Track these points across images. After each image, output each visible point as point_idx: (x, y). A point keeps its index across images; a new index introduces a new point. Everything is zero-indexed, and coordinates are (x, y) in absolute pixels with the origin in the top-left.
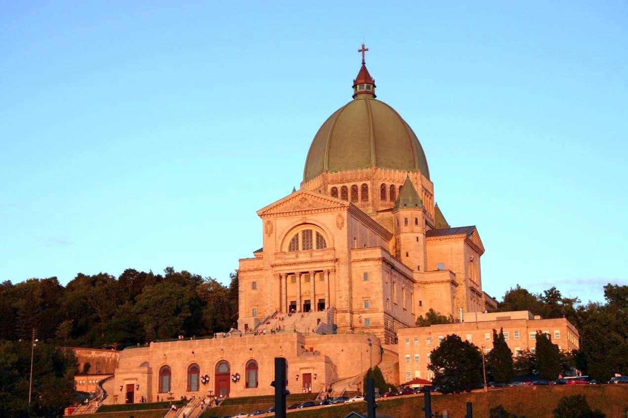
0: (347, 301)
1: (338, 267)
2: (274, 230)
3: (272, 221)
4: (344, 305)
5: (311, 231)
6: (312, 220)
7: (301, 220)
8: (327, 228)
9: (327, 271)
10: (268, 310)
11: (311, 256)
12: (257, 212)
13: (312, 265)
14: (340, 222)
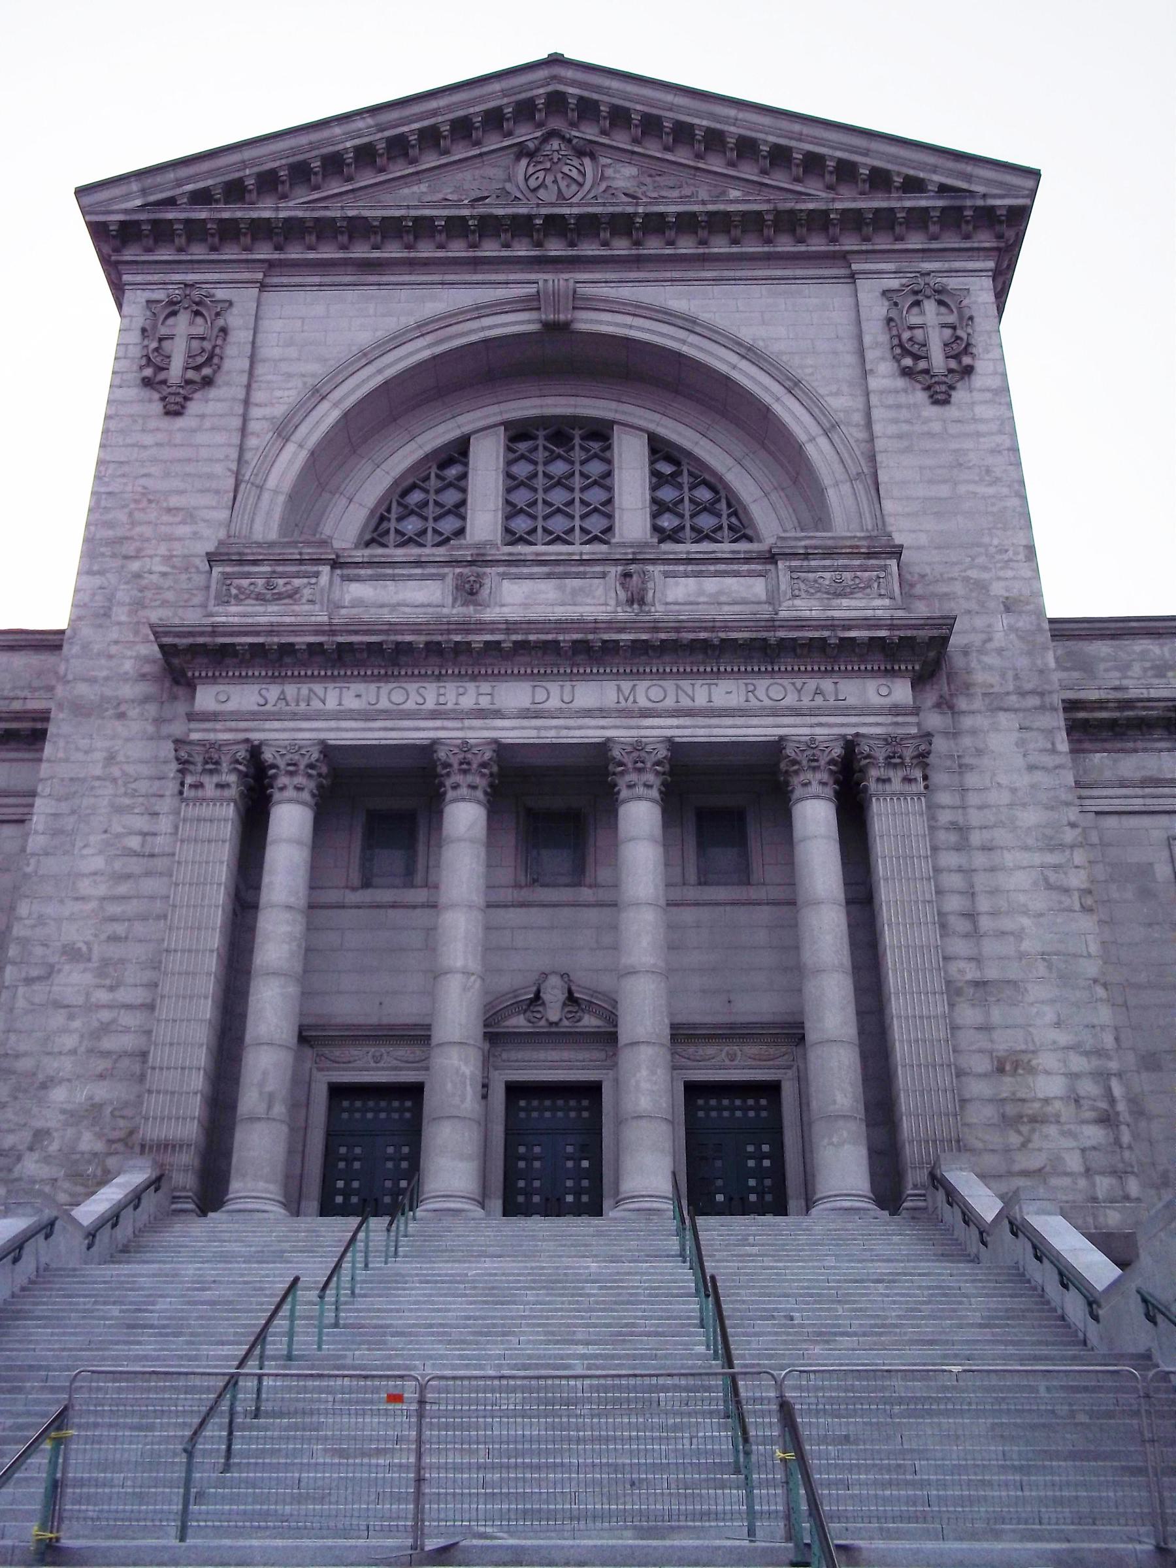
0: (1107, 1119)
2: (235, 361)
3: (220, 294)
4: (1074, 1162)
6: (638, 310)
7: (531, 303)
8: (793, 385)
9: (837, 751)
11: (637, 599)
12: (81, 192)
13: (646, 692)
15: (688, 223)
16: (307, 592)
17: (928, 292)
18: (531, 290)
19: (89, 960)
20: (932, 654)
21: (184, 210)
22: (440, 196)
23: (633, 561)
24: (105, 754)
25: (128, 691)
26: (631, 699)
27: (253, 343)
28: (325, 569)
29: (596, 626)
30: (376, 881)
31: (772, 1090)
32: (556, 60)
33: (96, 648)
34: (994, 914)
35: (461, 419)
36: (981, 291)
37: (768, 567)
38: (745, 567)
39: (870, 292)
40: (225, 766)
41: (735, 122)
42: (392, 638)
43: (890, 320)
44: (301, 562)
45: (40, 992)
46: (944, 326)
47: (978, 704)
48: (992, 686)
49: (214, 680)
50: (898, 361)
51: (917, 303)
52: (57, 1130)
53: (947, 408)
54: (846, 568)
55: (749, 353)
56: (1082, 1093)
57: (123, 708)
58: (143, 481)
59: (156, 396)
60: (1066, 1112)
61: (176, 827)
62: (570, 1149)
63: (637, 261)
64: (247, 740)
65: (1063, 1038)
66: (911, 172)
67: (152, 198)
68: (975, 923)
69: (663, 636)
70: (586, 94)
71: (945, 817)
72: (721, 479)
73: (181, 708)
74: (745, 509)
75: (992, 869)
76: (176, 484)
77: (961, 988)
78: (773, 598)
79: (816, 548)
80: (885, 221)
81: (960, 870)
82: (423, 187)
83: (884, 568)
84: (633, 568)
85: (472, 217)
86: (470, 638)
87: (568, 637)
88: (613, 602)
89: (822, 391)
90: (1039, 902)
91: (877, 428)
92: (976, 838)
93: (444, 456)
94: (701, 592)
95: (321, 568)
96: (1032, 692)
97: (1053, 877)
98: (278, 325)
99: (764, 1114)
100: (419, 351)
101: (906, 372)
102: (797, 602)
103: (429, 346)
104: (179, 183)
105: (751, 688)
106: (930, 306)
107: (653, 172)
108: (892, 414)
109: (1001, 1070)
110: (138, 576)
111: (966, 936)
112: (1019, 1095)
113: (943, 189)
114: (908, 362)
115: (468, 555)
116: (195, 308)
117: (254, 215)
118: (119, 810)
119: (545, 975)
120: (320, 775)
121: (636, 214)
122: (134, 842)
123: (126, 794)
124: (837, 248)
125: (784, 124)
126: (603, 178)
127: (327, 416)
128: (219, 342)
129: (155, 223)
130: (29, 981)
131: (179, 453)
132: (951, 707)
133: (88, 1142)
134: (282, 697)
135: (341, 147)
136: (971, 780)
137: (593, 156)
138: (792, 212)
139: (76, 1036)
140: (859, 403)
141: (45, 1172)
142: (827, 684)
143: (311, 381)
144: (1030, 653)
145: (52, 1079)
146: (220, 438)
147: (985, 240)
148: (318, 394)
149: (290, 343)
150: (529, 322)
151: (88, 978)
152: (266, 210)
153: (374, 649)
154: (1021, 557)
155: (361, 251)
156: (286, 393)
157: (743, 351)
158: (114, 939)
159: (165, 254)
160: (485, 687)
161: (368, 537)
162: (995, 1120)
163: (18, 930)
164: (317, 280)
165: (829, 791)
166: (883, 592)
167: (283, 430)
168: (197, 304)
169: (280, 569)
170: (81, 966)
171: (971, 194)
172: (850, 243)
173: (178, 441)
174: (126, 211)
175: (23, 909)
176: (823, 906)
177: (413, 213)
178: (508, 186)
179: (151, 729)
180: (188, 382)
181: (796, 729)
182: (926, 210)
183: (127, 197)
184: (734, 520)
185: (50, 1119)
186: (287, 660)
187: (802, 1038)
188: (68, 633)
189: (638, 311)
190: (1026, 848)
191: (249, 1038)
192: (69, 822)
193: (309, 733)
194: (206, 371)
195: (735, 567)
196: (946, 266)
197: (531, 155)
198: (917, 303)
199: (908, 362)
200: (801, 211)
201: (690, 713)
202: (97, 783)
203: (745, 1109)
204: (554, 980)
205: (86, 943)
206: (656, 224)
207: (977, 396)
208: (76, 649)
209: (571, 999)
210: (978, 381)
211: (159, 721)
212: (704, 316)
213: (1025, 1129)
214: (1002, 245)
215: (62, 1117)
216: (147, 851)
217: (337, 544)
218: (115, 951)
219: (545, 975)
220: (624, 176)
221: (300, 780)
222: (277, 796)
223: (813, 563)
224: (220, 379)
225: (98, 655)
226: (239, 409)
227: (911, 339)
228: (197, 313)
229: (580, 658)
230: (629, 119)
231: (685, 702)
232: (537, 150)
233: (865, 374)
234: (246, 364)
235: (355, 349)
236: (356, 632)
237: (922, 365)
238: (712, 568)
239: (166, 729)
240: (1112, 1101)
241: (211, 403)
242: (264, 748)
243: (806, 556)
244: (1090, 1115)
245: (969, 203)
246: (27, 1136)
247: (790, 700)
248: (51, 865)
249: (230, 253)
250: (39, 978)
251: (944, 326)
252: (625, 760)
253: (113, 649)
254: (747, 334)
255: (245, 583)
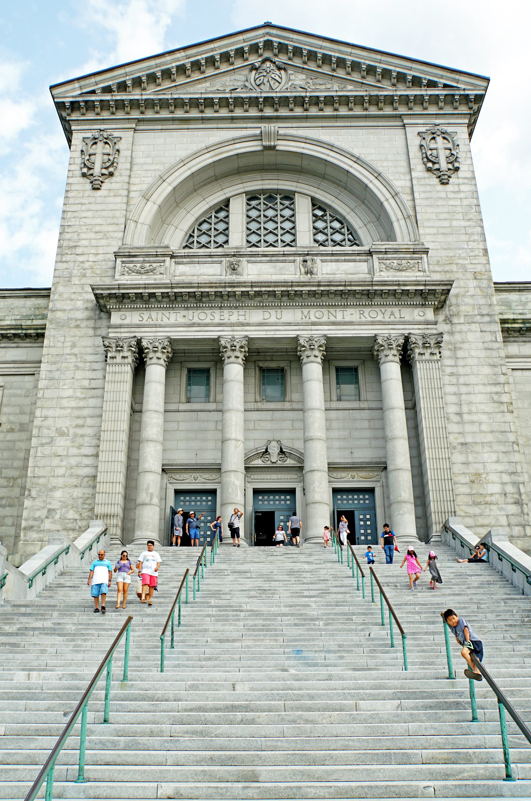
0: (517, 503)
1: (451, 333)
2: (123, 164)
3: (116, 134)
4: (504, 521)
5: (289, 196)
7: (259, 138)
8: (378, 176)
9: (401, 341)
10: (47, 525)
12: (52, 88)
13: (314, 314)
14: (443, 155)
15: (330, 101)
16: (158, 270)
17: (439, 133)
18: (258, 132)
19: (68, 435)
20: (443, 297)
21: (99, 96)
22: (216, 88)
23: (308, 254)
24: (71, 344)
25: (81, 315)
26: (308, 317)
27: (131, 156)
28: (168, 259)
29: (292, 284)
30: (192, 400)
31: (371, 491)
32: (268, 25)
33: (65, 296)
34: (470, 413)
35: (226, 191)
36: (462, 132)
37: (369, 257)
38: (358, 258)
39: (412, 132)
40: (125, 348)
41: (350, 54)
42: (200, 290)
43: (421, 146)
44: (157, 256)
45: (47, 450)
46: (446, 149)
47: (462, 320)
48: (468, 312)
49: (119, 309)
50: (425, 165)
51: (434, 138)
52: (58, 509)
53: (447, 186)
54: (404, 259)
55: (358, 160)
56: (507, 491)
57: (78, 322)
58: (84, 220)
59: (89, 181)
60: (501, 499)
61: (105, 377)
62: (282, 518)
63: (307, 118)
64: (135, 337)
65: (500, 467)
66: (431, 78)
67: (84, 91)
68: (461, 417)
69: (322, 288)
70: (282, 41)
71: (448, 370)
72: (344, 218)
73: (104, 322)
74: (355, 231)
75: (469, 394)
76: (99, 221)
77: (455, 446)
78: (371, 271)
79: (390, 249)
80: (419, 100)
81: (455, 394)
82: (208, 84)
83: (421, 258)
84: (307, 258)
85: (231, 98)
86: (235, 289)
87: (279, 289)
88: (299, 273)
89: (391, 178)
90: (490, 407)
91: (416, 195)
92: (462, 380)
93: (218, 208)
94: (338, 269)
95: (166, 258)
96: (488, 315)
97: (496, 397)
98: (143, 148)
99: (367, 502)
100: (207, 159)
101: (429, 170)
102: (382, 273)
103: (211, 157)
104: (97, 83)
105: (362, 312)
106: (439, 139)
107: (313, 77)
108: (422, 189)
109: (473, 482)
110: (83, 262)
111: (458, 423)
112: (481, 492)
113: (445, 86)
114: (430, 165)
115: (232, 251)
116: (105, 140)
117: (132, 97)
118: (77, 368)
119: (270, 441)
120: (168, 352)
121: (306, 97)
122: (86, 383)
123: (81, 362)
124: (397, 113)
125: (374, 56)
126: (290, 80)
127: (166, 189)
128: (116, 156)
129: (86, 102)
130: (42, 445)
131: (100, 207)
132: (451, 322)
133: (72, 514)
134: (150, 317)
135: (169, 66)
136: (460, 354)
137: (285, 70)
138: (377, 96)
139: (64, 469)
140: (408, 184)
141: (54, 527)
142: (396, 310)
143: (158, 173)
144: (485, 297)
145: (55, 487)
146: (118, 200)
147: (463, 109)
148: (162, 179)
149: (148, 156)
150: (257, 146)
151: (68, 443)
152: (136, 95)
153: (192, 295)
154: (481, 254)
155: (179, 114)
156: (147, 179)
157: (355, 159)
158: (77, 426)
159: (90, 116)
160: (242, 312)
161: (184, 244)
162: (471, 503)
163: (37, 422)
164: (160, 127)
165: (397, 359)
166: (420, 269)
167: (146, 197)
168: (106, 139)
169: (147, 259)
170: (65, 438)
171: (458, 88)
172: (402, 110)
173: (99, 202)
174: (73, 97)
175: (38, 413)
176: (395, 410)
177: (204, 96)
178: (247, 84)
179: (91, 332)
180: (103, 175)
181: (382, 332)
182: (438, 95)
183: (74, 90)
184: (350, 236)
185: (55, 505)
186: (152, 300)
187: (385, 468)
188: (52, 289)
189: (307, 141)
190: (484, 384)
191: (141, 469)
192: (56, 375)
193: (162, 334)
194: (111, 169)
195: (353, 258)
196: (446, 121)
197: (256, 69)
198: (434, 138)
199: (430, 165)
200: (381, 95)
201: (334, 324)
202: (68, 357)
203: (358, 500)
204: (274, 444)
205: (66, 427)
206: (315, 101)
207: (461, 181)
208: (56, 297)
209: (282, 452)
210: (460, 174)
211: (95, 328)
212: (337, 144)
213: (482, 507)
214: (472, 112)
215: (60, 504)
216: (92, 386)
217: (172, 248)
218: (80, 431)
219: (270, 441)
220: (299, 79)
221: (159, 355)
222: (148, 362)
223: (389, 256)
224: (116, 173)
225: (66, 299)
226: (126, 186)
227: (431, 155)
228: (106, 143)
229: (285, 299)
230: (302, 53)
231: (332, 319)
232: (260, 67)
233: (410, 171)
234: (128, 166)
235: (178, 159)
236: (183, 287)
237: (436, 166)
238: (343, 258)
239: (99, 332)
240: (520, 494)
241: (113, 185)
242: (143, 340)
243: (386, 253)
244: (512, 500)
245: (457, 92)
246: (45, 512)
247: (380, 318)
248: (48, 394)
249: (120, 115)
250: (47, 443)
251: (446, 149)
252: (306, 345)
253: (73, 296)
254: (356, 152)
255: (131, 265)
